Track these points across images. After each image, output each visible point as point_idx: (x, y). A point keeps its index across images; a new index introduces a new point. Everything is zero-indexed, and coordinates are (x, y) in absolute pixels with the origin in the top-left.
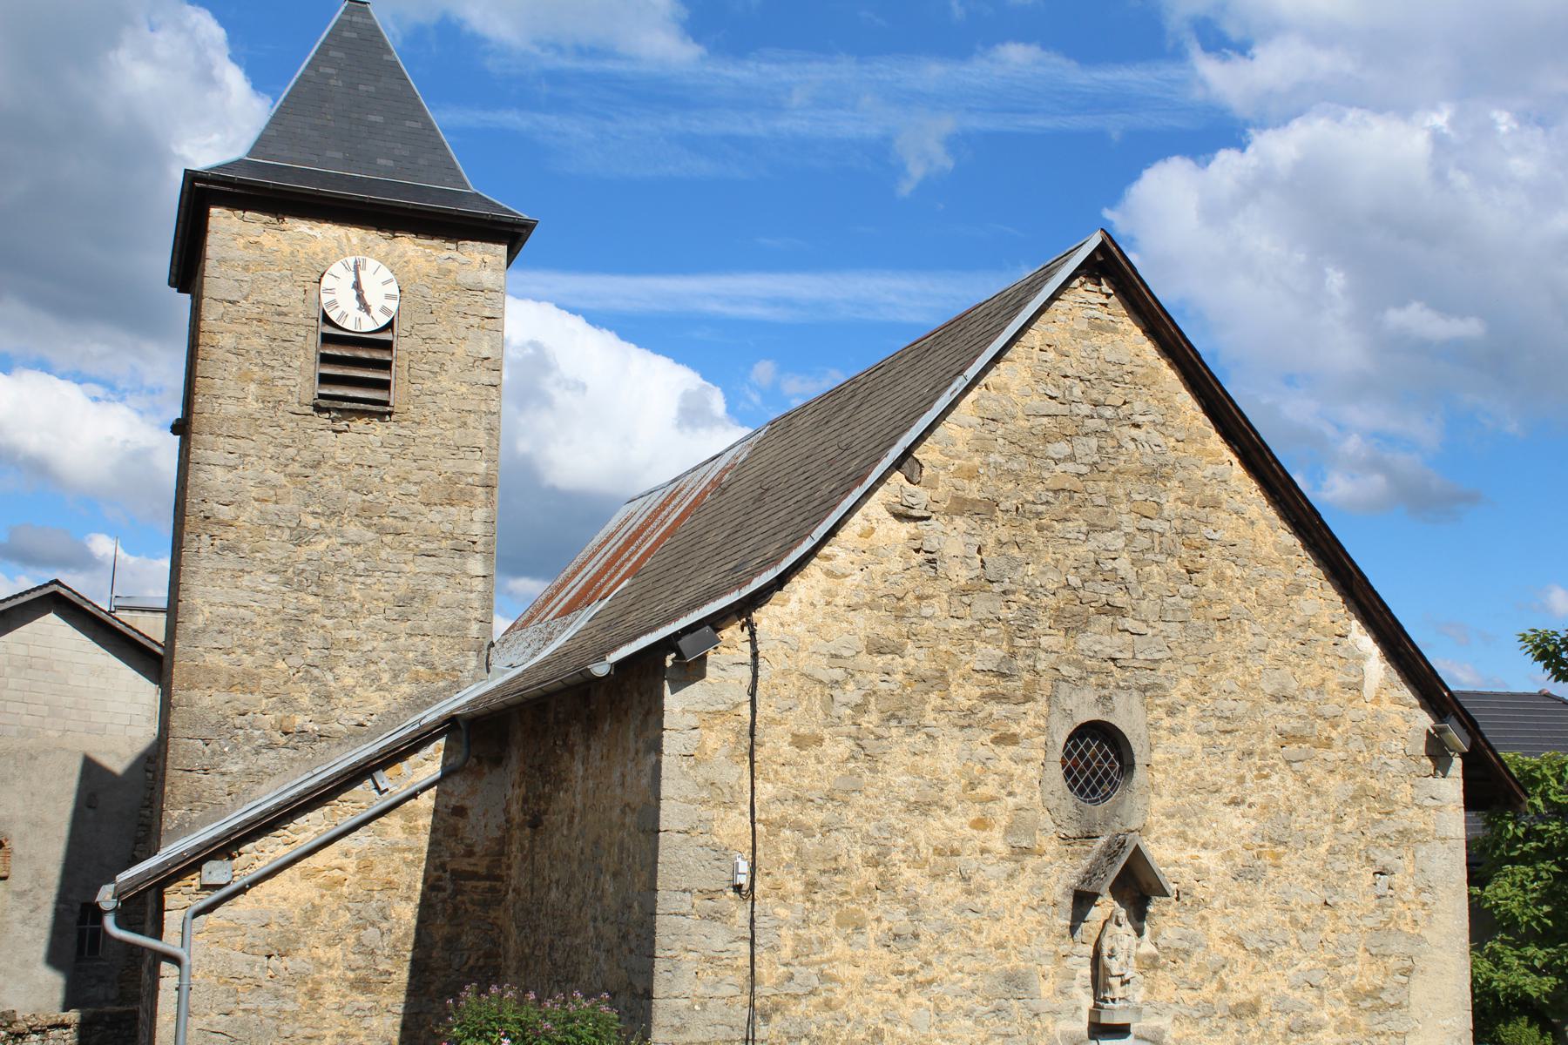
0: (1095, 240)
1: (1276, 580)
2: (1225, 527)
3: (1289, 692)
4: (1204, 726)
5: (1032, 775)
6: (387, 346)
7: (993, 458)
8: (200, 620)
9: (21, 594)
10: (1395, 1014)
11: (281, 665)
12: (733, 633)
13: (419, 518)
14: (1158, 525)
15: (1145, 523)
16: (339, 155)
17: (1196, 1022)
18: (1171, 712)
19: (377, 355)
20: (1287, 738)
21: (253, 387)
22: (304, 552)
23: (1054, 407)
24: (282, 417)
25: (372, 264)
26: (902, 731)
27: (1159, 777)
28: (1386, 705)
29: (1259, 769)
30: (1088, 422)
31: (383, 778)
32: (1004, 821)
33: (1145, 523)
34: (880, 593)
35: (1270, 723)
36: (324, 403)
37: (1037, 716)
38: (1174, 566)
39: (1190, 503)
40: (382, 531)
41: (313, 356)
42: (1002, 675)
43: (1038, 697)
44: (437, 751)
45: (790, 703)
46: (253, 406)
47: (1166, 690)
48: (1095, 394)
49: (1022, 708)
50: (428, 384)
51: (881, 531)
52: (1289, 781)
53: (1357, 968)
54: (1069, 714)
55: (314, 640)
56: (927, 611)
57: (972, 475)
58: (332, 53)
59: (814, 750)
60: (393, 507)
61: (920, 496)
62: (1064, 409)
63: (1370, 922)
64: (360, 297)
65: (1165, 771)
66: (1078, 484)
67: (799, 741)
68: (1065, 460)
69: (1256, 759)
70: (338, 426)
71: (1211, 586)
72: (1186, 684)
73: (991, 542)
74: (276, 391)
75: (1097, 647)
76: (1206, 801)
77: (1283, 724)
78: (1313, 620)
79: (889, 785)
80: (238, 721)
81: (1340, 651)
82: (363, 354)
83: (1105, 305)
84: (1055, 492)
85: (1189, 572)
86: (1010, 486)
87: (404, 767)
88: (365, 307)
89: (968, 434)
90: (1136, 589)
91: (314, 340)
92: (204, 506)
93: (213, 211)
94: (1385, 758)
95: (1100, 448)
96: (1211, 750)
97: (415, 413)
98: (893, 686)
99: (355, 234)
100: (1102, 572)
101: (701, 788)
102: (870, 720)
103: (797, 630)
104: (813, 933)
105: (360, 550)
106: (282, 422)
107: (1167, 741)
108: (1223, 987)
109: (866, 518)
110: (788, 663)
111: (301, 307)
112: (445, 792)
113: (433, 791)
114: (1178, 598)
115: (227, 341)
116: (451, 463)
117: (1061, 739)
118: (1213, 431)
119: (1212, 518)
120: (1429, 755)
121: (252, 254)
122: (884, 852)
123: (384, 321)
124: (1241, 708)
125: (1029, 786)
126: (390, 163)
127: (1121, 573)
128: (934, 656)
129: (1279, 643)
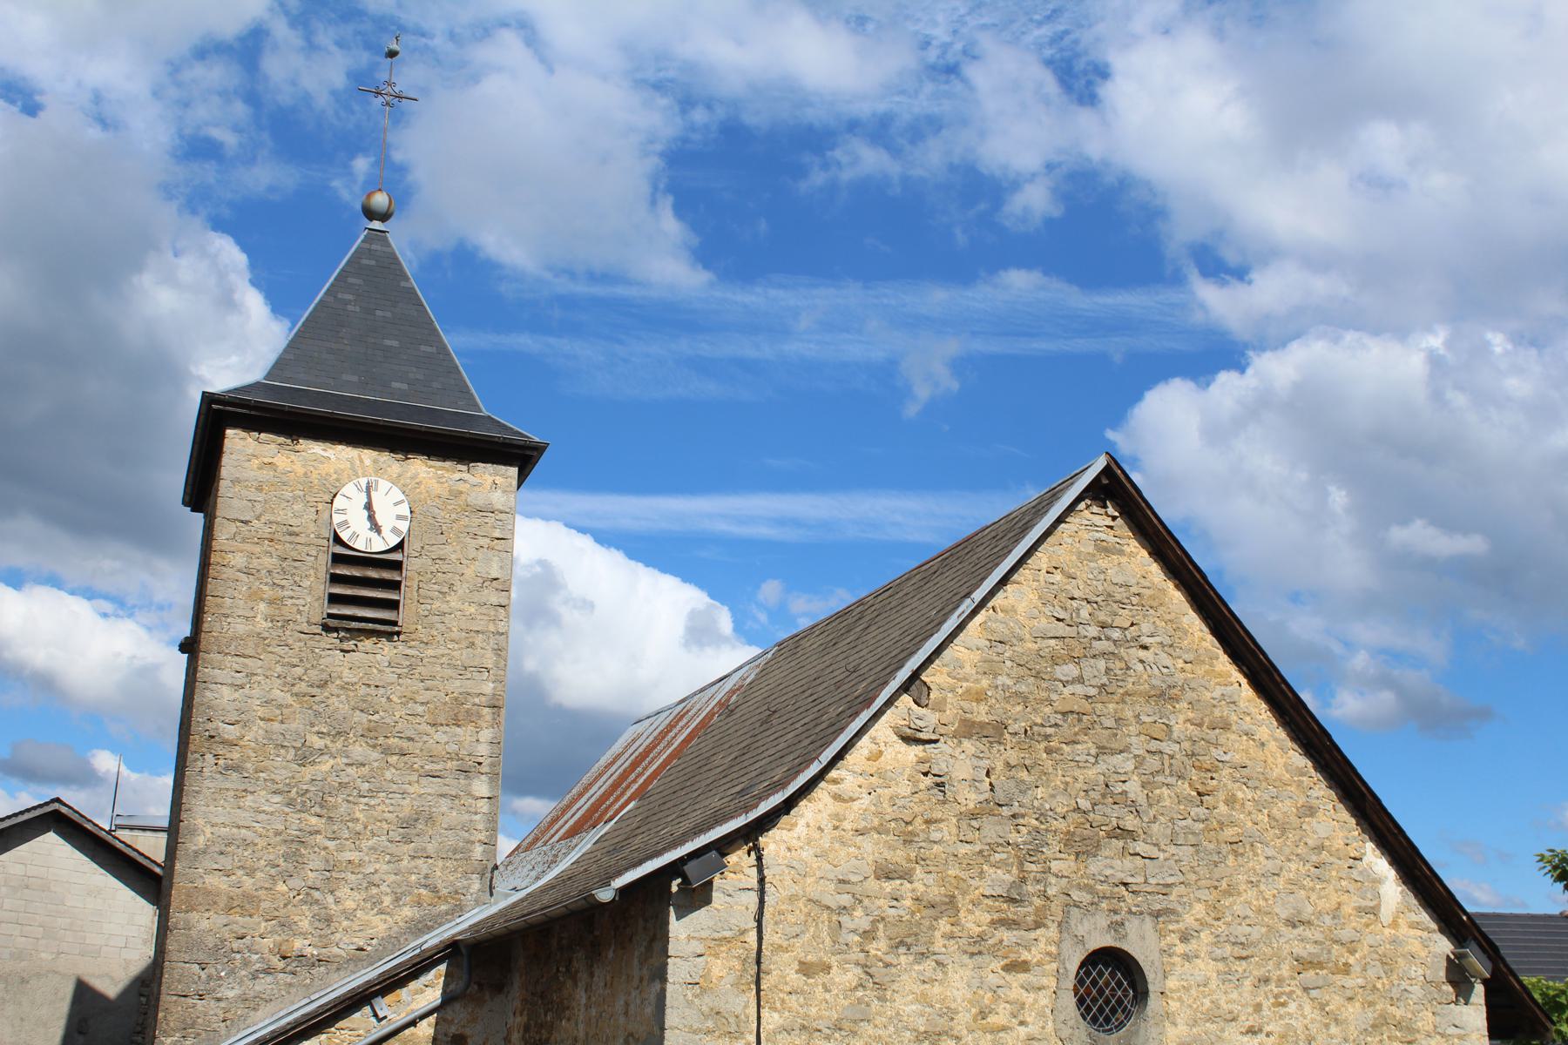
0: (1100, 463)
1: (1288, 802)
2: (1235, 748)
3: (1305, 917)
4: (1218, 952)
6: (397, 566)
7: (1002, 680)
8: (201, 841)
9: (22, 813)
11: (281, 887)
12: (739, 858)
13: (425, 738)
14: (1168, 747)
15: (1154, 745)
16: (355, 379)
18: (1185, 938)
19: (387, 575)
20: (1303, 964)
21: (262, 606)
22: (308, 772)
23: (1061, 629)
24: (290, 636)
25: (384, 485)
26: (911, 958)
27: (1174, 1005)
28: (1404, 930)
29: (1276, 997)
30: (1096, 644)
31: (383, 1005)
33: (1154, 745)
34: (888, 817)
35: (1286, 949)
36: (333, 623)
37: (1048, 942)
38: (1184, 788)
39: (1200, 725)
40: (387, 751)
41: (323, 575)
42: (1013, 900)
43: (1049, 923)
44: (437, 977)
45: (797, 929)
46: (262, 625)
47: (1179, 915)
48: (1102, 616)
49: (1033, 935)
50: (437, 604)
51: (889, 754)
52: (1307, 1009)
54: (1081, 941)
55: (316, 862)
56: (935, 836)
57: (980, 697)
58: (351, 280)
59: (821, 978)
60: (399, 727)
61: (928, 719)
62: (1071, 631)
64: (371, 518)
65: (1180, 999)
66: (1087, 706)
67: (806, 969)
68: (1073, 682)
69: (1272, 986)
70: (346, 646)
71: (1223, 808)
72: (1199, 909)
73: (999, 766)
74: (285, 610)
75: (1108, 872)
76: (1223, 1030)
77: (1299, 950)
78: (1327, 843)
79: (898, 1014)
80: (236, 945)
81: (1355, 874)
82: (373, 574)
83: (1111, 527)
84: (1064, 714)
85: (1199, 794)
86: (1019, 708)
87: (403, 993)
88: (376, 528)
89: (976, 657)
90: (1146, 813)
91: (324, 560)
92: (210, 726)
93: (229, 432)
94: (1404, 985)
95: (1108, 670)
96: (1226, 976)
97: (423, 634)
98: (902, 913)
99: (368, 456)
100: (1112, 794)
101: (706, 1017)
102: (879, 947)
103: (804, 854)
105: (365, 770)
106: (290, 642)
109: (874, 741)
110: (796, 889)
111: (312, 527)
112: (445, 1020)
113: (432, 1019)
114: (1189, 821)
115: (238, 560)
116: (458, 683)
117: (1073, 966)
118: (1221, 652)
119: (1222, 740)
120: (1451, 982)
121: (266, 474)
123: (394, 541)
124: (1257, 933)
125: (1042, 1015)
126: (405, 386)
127: (1132, 796)
128: (943, 881)
129: (1293, 866)
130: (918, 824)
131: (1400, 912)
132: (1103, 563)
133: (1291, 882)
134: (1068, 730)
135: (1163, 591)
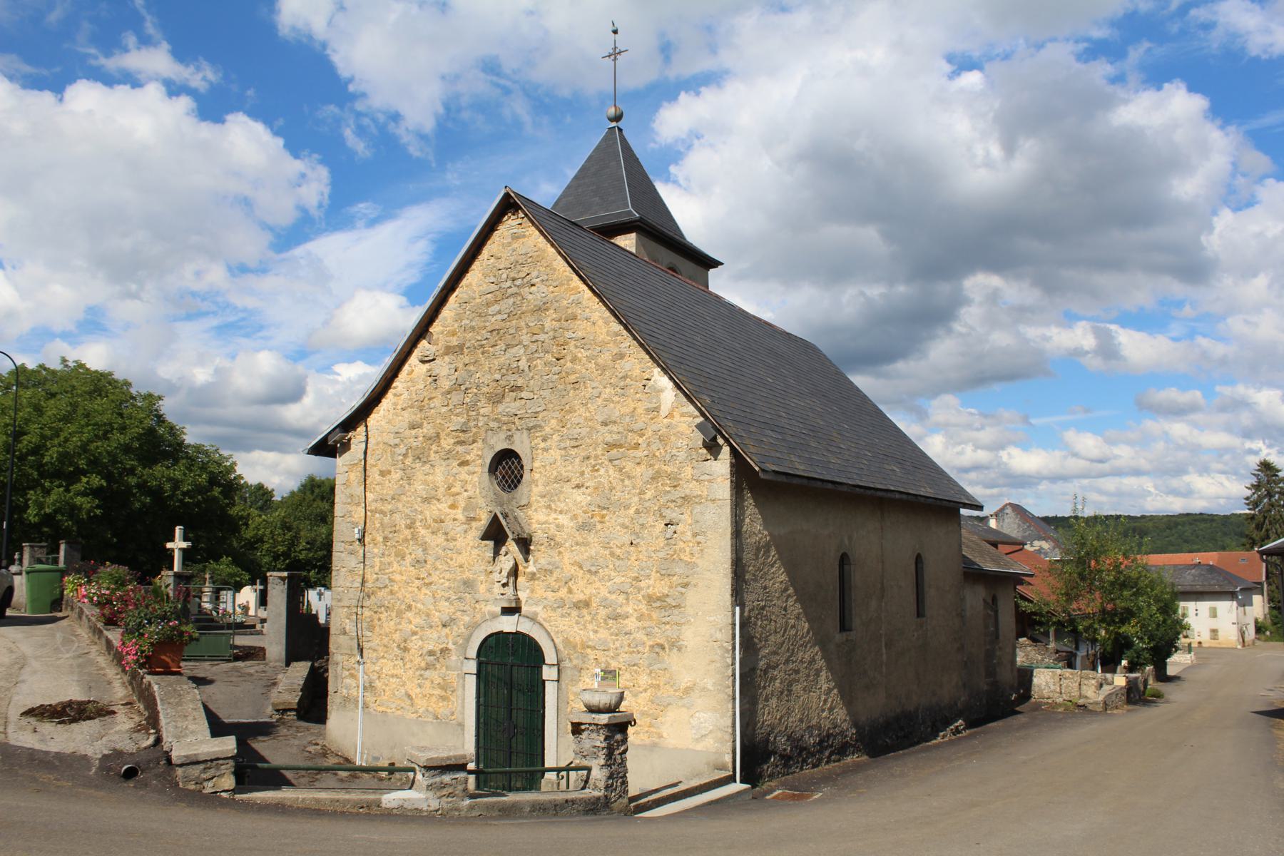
2: (581, 328)
3: (613, 419)
4: (563, 445)
5: (475, 482)
7: (466, 322)
10: (676, 611)
12: (361, 429)
14: (542, 337)
15: (535, 337)
17: (554, 610)
18: (544, 440)
20: (611, 446)
23: (493, 287)
27: (537, 476)
28: (677, 417)
32: (462, 504)
33: (535, 337)
38: (549, 357)
48: (512, 275)
51: (416, 370)
52: (611, 472)
53: (651, 582)
57: (454, 334)
59: (388, 477)
62: (497, 287)
63: (661, 555)
67: (382, 474)
71: (569, 364)
72: (554, 422)
73: (461, 365)
77: (609, 439)
94: (674, 452)
96: (565, 458)
102: (409, 461)
104: (386, 560)
107: (540, 455)
108: (570, 591)
117: (488, 461)
122: (413, 522)
124: (584, 431)
125: (474, 486)
129: (607, 391)
130: (426, 401)
131: (673, 410)
132: (515, 245)
133: (606, 400)
134: (492, 341)
135: (544, 251)
